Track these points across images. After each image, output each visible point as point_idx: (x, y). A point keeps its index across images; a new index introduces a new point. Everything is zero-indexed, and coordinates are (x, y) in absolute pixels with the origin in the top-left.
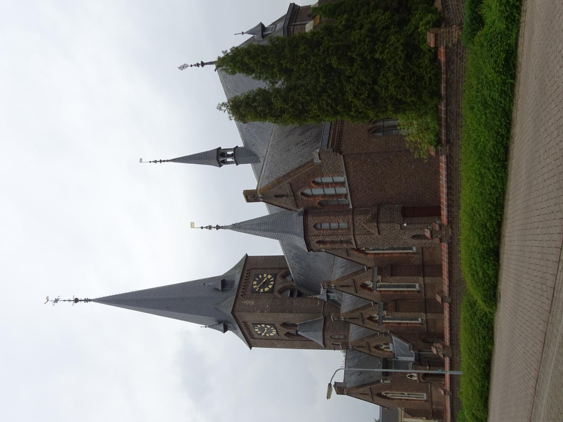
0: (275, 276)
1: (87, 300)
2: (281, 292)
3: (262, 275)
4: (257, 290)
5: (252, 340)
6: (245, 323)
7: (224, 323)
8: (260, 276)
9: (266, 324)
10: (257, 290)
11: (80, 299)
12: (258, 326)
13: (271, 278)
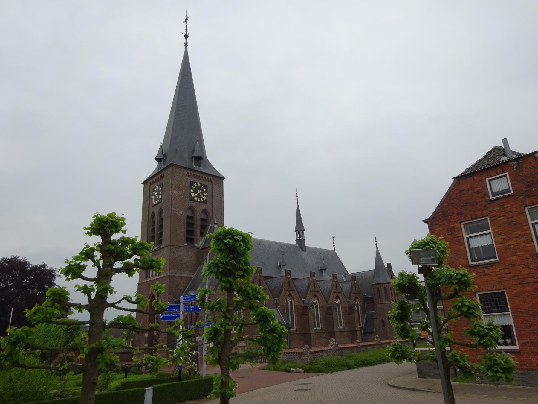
0: (205, 202)
1: (186, 45)
2: (191, 208)
3: (206, 192)
4: (192, 187)
5: (149, 183)
6: (163, 177)
7: (163, 158)
9: (162, 195)
10: (192, 187)
11: (187, 39)
12: (161, 188)
13: (203, 199)
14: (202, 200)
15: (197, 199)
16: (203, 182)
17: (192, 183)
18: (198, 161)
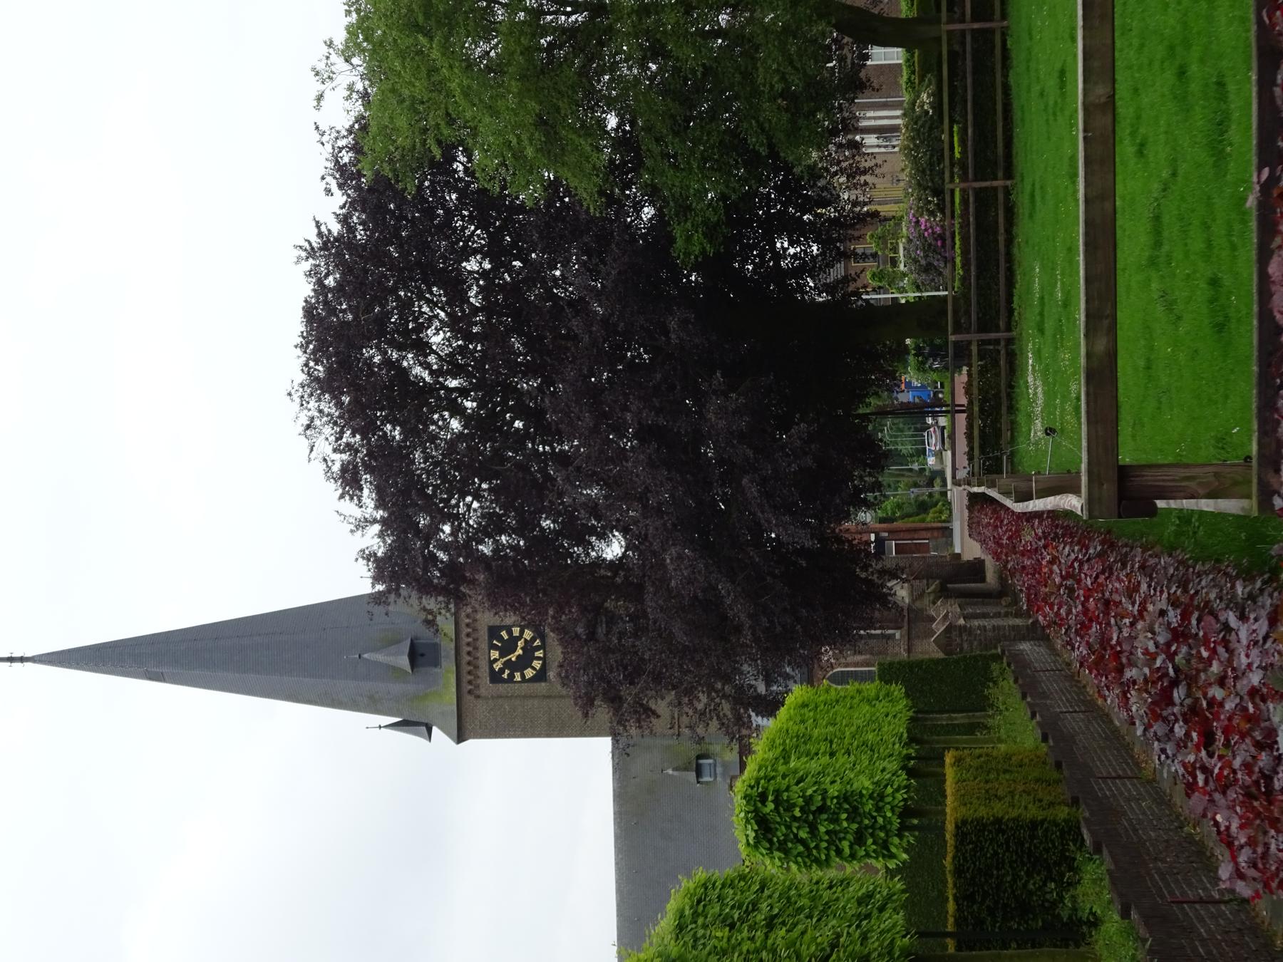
4: (505, 676)
8: (504, 634)
10: (505, 676)
13: (533, 639)
14: (537, 643)
15: (538, 658)
16: (483, 645)
17: (495, 677)
18: (422, 655)
